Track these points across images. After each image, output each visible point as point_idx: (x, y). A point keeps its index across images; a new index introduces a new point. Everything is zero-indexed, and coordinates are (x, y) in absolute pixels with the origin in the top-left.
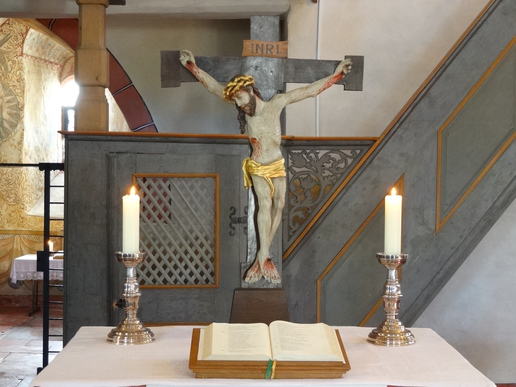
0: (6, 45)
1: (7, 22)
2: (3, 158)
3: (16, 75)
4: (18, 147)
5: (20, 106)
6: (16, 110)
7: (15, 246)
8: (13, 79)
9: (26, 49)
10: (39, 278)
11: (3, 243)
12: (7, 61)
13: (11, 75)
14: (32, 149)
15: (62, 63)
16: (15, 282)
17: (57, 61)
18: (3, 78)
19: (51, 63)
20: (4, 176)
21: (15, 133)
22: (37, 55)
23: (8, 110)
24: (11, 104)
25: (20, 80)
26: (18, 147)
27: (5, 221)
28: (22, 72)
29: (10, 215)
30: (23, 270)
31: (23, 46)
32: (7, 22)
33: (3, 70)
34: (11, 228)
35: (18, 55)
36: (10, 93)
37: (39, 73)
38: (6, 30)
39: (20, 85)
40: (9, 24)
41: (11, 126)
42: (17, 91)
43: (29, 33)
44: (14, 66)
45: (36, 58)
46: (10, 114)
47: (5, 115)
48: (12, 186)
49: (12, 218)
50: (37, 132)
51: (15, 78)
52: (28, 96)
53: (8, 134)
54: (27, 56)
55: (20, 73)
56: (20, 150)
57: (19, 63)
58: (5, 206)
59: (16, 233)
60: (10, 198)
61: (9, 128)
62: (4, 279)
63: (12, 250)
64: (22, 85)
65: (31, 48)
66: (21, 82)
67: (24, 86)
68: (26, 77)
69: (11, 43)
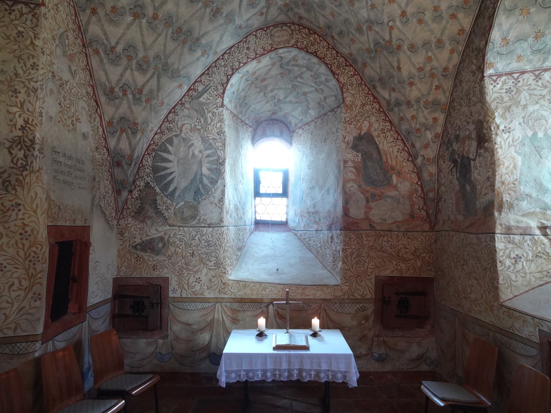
0: (205, 96)
1: (206, 72)
2: (202, 217)
3: (216, 127)
4: (218, 205)
5: (221, 161)
6: (216, 164)
7: (216, 316)
8: (213, 131)
9: (226, 101)
10: (256, 379)
11: (203, 313)
12: (206, 113)
13: (210, 127)
14: (232, 206)
15: (255, 126)
16: (224, 386)
17: (251, 124)
18: (202, 130)
19: (247, 124)
20: (204, 237)
21: (215, 190)
22: (235, 112)
23: (208, 165)
24: (211, 159)
25: (221, 132)
26: (218, 205)
27: (205, 287)
28: (222, 124)
29: (210, 280)
30: (235, 368)
31: (223, 97)
32: (206, 72)
33: (202, 122)
34: (212, 296)
35: (219, 106)
36: (210, 146)
37: (237, 131)
38: (206, 81)
39: (221, 138)
40: (208, 74)
41: (211, 182)
42: (217, 144)
43: (230, 83)
44: (214, 118)
45: (234, 115)
46: (209, 169)
47: (205, 171)
48: (213, 248)
49: (213, 284)
50: (236, 190)
51: (215, 131)
52: (229, 149)
53: (207, 191)
54: (227, 109)
55: (221, 126)
56: (221, 208)
57: (219, 115)
58: (205, 271)
59: (217, 300)
60: (210, 261)
61: (209, 185)
62: (204, 355)
63: (213, 320)
64: (223, 138)
65: (230, 101)
66: (222, 134)
67: (225, 139)
68: (226, 129)
69: (210, 94)
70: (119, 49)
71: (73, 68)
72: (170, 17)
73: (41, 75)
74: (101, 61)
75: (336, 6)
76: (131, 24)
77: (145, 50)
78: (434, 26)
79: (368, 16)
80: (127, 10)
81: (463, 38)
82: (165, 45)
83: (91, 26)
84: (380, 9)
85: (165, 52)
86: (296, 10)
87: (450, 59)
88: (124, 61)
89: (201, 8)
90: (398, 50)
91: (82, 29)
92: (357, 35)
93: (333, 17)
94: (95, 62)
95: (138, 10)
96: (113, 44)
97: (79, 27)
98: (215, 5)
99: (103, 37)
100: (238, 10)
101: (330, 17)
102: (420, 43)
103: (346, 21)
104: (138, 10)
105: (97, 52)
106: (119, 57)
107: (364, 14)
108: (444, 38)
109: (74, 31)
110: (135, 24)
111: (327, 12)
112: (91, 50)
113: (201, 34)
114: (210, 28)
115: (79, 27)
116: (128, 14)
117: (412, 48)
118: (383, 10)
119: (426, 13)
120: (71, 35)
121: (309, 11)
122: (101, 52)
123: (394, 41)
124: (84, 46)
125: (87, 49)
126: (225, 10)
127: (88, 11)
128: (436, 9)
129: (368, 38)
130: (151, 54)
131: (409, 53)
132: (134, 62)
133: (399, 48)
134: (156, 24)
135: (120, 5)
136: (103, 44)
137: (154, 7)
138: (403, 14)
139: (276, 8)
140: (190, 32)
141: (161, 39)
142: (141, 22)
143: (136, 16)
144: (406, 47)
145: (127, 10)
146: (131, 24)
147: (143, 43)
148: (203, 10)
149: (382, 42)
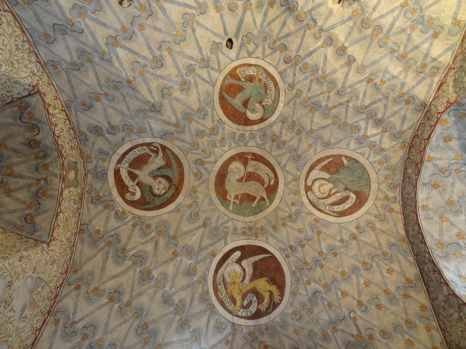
70: (80, 325)
71: (27, 312)
72: (142, 309)
73: (3, 265)
74: (55, 332)
75: (297, 320)
76: (104, 305)
77: (105, 332)
78: (394, 308)
79: (329, 317)
80: (107, 293)
81: (429, 313)
82: (126, 336)
83: (67, 298)
84: (336, 304)
85: (123, 344)
86: (261, 338)
87: (432, 338)
88: (77, 339)
89: (171, 313)
90: (371, 339)
91: (58, 299)
92: (325, 344)
93: (297, 334)
94: (48, 331)
95: (116, 295)
96: (77, 319)
97: (57, 296)
98: (184, 315)
99: (72, 310)
100: (205, 329)
101: (294, 336)
102: (390, 328)
103: (311, 334)
104: (116, 295)
105: (56, 322)
106: (75, 333)
107: (324, 316)
108: (411, 317)
109: (51, 292)
110: (107, 306)
111: (290, 331)
112: (52, 318)
113: (165, 341)
114: (175, 339)
115: (57, 296)
116: (106, 296)
117: (384, 334)
118: (340, 305)
119: (380, 297)
120: (46, 291)
121: (273, 335)
122: (61, 324)
123: (363, 331)
124: (49, 312)
125: (49, 317)
126: (194, 324)
127: (73, 287)
128: (387, 292)
129: (337, 342)
130: (109, 338)
131: (384, 341)
132: (87, 342)
133: (371, 337)
134: (127, 311)
135: (103, 288)
136: (68, 316)
137: (131, 297)
138: (360, 303)
139: (242, 336)
140: (154, 333)
141: (125, 327)
142: (114, 306)
143: (111, 300)
144: (378, 335)
145: (107, 293)
146: (104, 305)
147: (106, 325)
148: (173, 315)
149: (352, 339)
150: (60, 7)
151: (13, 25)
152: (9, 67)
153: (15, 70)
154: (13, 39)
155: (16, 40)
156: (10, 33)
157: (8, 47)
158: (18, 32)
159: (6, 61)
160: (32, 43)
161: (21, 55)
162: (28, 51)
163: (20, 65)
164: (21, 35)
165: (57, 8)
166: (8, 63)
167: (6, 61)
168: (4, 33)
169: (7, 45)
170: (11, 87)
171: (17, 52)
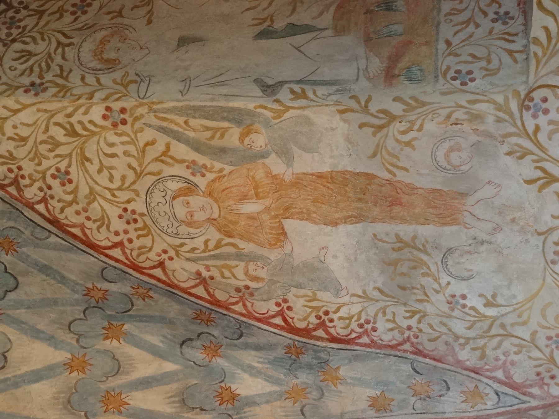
150: (36, 334)
151: (88, 224)
152: (80, 122)
153: (60, 118)
154: (84, 190)
155: (75, 192)
156: (95, 204)
157: (93, 168)
158: (70, 216)
159: (94, 134)
160: (20, 206)
161: (46, 164)
162: (23, 182)
163: (42, 137)
164: (57, 211)
165: (41, 327)
166: (85, 129)
167: (94, 134)
168: (114, 195)
169: (100, 171)
170: (36, 69)
171: (63, 166)
